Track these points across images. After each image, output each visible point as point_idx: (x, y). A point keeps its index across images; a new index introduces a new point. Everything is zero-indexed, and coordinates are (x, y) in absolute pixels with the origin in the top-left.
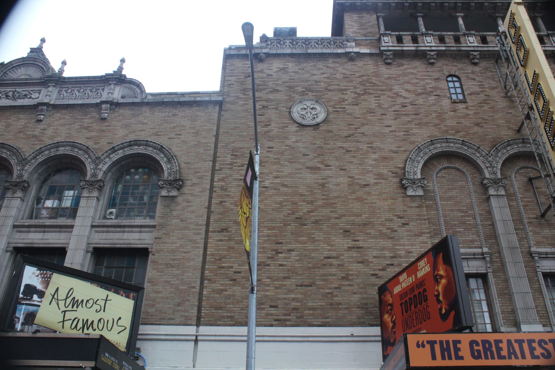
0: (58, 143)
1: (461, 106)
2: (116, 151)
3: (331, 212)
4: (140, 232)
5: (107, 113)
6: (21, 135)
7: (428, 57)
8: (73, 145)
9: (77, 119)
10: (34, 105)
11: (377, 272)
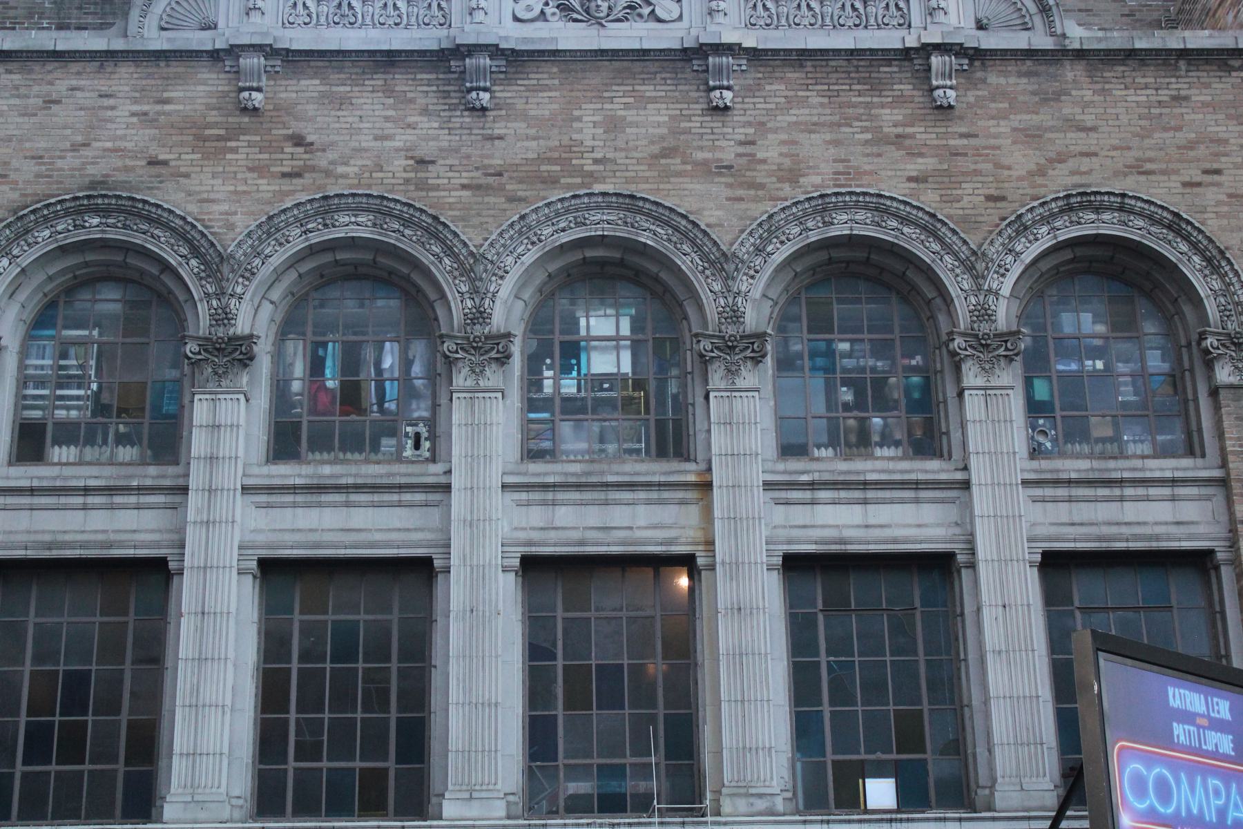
0: (822, 196)
2: (1026, 228)
4: (1173, 499)
5: (951, 88)
6: (675, 163)
8: (880, 206)
9: (854, 106)
10: (685, 50)
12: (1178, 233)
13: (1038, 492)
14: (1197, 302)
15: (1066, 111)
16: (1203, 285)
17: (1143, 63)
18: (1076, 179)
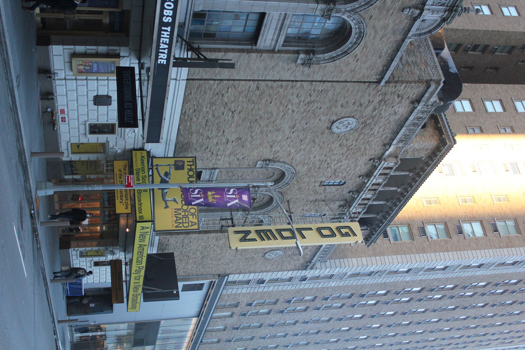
1: (317, 184)
3: (257, 133)
4: (272, 40)
7: (365, 178)
11: (209, 149)
12: (344, 53)
13: (282, 16)
14: (324, 52)
15: (389, 35)
16: (327, 55)
17: (394, 51)
18: (368, 34)
